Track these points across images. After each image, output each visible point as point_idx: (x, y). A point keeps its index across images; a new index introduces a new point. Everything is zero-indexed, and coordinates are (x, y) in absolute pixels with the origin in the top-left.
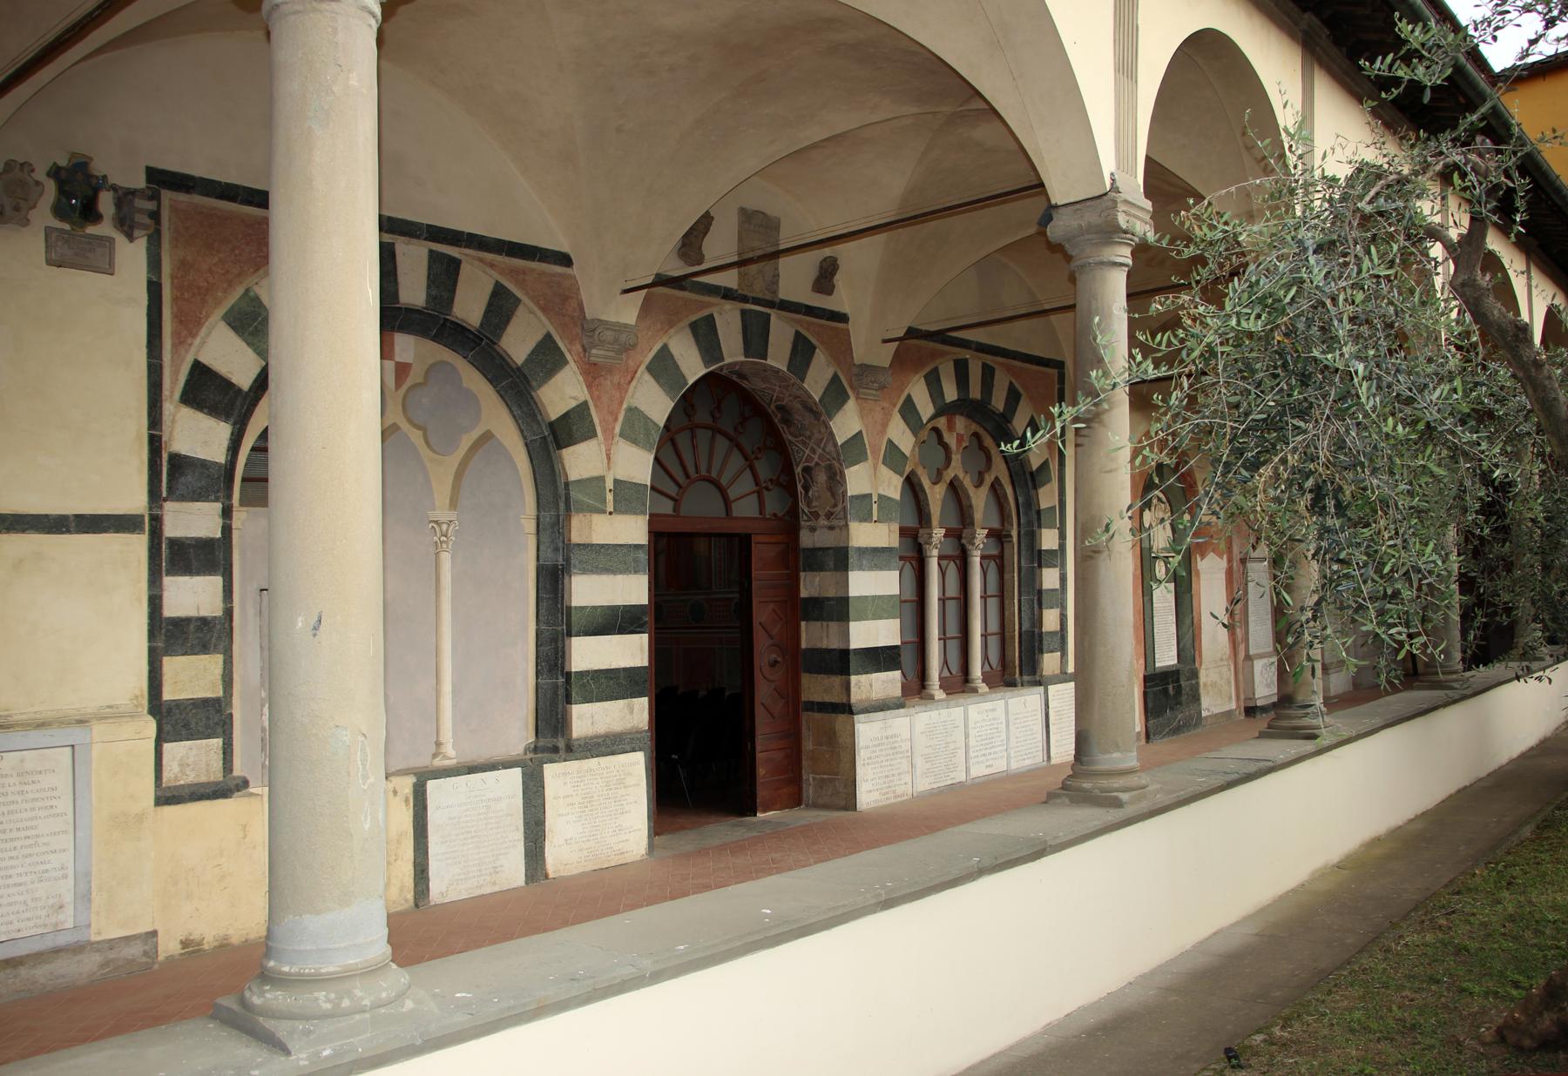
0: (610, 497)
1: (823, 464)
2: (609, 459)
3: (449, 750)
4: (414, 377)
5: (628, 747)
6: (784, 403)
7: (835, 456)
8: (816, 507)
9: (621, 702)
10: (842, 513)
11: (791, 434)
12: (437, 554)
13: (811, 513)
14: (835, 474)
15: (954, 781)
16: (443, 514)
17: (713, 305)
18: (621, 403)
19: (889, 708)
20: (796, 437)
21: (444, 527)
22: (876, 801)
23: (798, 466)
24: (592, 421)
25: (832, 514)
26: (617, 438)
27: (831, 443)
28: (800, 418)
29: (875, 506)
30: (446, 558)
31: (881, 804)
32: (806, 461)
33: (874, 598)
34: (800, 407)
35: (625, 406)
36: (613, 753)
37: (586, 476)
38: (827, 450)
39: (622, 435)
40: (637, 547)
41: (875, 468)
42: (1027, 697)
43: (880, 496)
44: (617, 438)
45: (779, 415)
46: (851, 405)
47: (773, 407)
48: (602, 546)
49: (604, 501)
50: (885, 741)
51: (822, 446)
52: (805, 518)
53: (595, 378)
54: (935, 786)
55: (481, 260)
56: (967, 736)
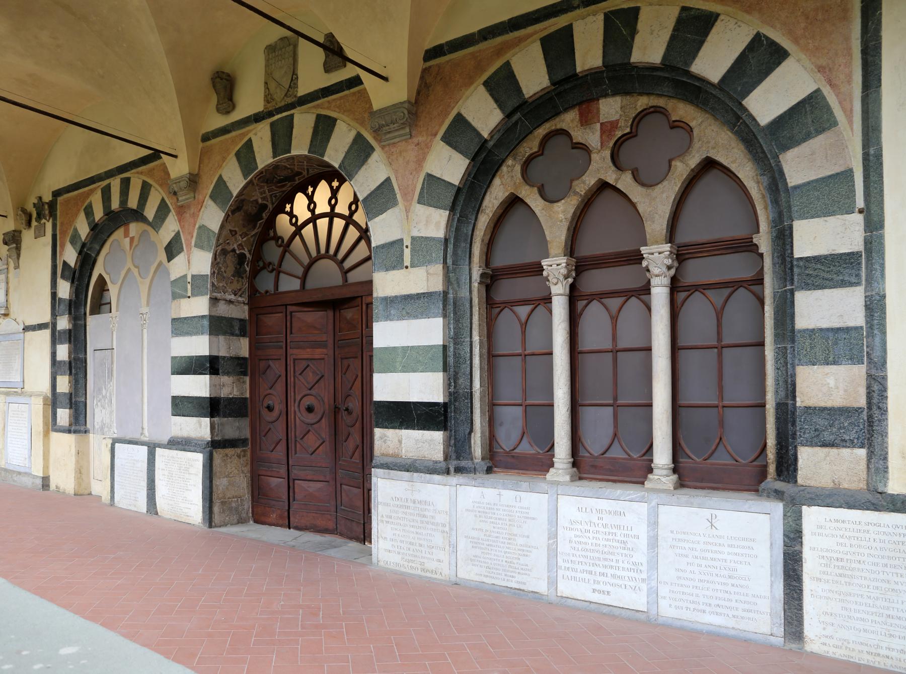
0: (189, 286)
2: (189, 263)
3: (146, 432)
4: (136, 240)
5: (192, 449)
9: (195, 419)
12: (142, 330)
15: (522, 587)
16: (144, 310)
17: (250, 131)
18: (195, 225)
19: (417, 470)
21: (145, 315)
22: (397, 564)
24: (181, 242)
26: (193, 248)
30: (145, 331)
31: (403, 569)
33: (405, 349)
35: (197, 226)
36: (185, 450)
37: (178, 276)
39: (196, 246)
40: (203, 317)
43: (414, 239)
44: (193, 248)
48: (185, 318)
49: (186, 290)
50: (411, 505)
53: (181, 215)
54: (488, 581)
55: (138, 173)
56: (553, 536)
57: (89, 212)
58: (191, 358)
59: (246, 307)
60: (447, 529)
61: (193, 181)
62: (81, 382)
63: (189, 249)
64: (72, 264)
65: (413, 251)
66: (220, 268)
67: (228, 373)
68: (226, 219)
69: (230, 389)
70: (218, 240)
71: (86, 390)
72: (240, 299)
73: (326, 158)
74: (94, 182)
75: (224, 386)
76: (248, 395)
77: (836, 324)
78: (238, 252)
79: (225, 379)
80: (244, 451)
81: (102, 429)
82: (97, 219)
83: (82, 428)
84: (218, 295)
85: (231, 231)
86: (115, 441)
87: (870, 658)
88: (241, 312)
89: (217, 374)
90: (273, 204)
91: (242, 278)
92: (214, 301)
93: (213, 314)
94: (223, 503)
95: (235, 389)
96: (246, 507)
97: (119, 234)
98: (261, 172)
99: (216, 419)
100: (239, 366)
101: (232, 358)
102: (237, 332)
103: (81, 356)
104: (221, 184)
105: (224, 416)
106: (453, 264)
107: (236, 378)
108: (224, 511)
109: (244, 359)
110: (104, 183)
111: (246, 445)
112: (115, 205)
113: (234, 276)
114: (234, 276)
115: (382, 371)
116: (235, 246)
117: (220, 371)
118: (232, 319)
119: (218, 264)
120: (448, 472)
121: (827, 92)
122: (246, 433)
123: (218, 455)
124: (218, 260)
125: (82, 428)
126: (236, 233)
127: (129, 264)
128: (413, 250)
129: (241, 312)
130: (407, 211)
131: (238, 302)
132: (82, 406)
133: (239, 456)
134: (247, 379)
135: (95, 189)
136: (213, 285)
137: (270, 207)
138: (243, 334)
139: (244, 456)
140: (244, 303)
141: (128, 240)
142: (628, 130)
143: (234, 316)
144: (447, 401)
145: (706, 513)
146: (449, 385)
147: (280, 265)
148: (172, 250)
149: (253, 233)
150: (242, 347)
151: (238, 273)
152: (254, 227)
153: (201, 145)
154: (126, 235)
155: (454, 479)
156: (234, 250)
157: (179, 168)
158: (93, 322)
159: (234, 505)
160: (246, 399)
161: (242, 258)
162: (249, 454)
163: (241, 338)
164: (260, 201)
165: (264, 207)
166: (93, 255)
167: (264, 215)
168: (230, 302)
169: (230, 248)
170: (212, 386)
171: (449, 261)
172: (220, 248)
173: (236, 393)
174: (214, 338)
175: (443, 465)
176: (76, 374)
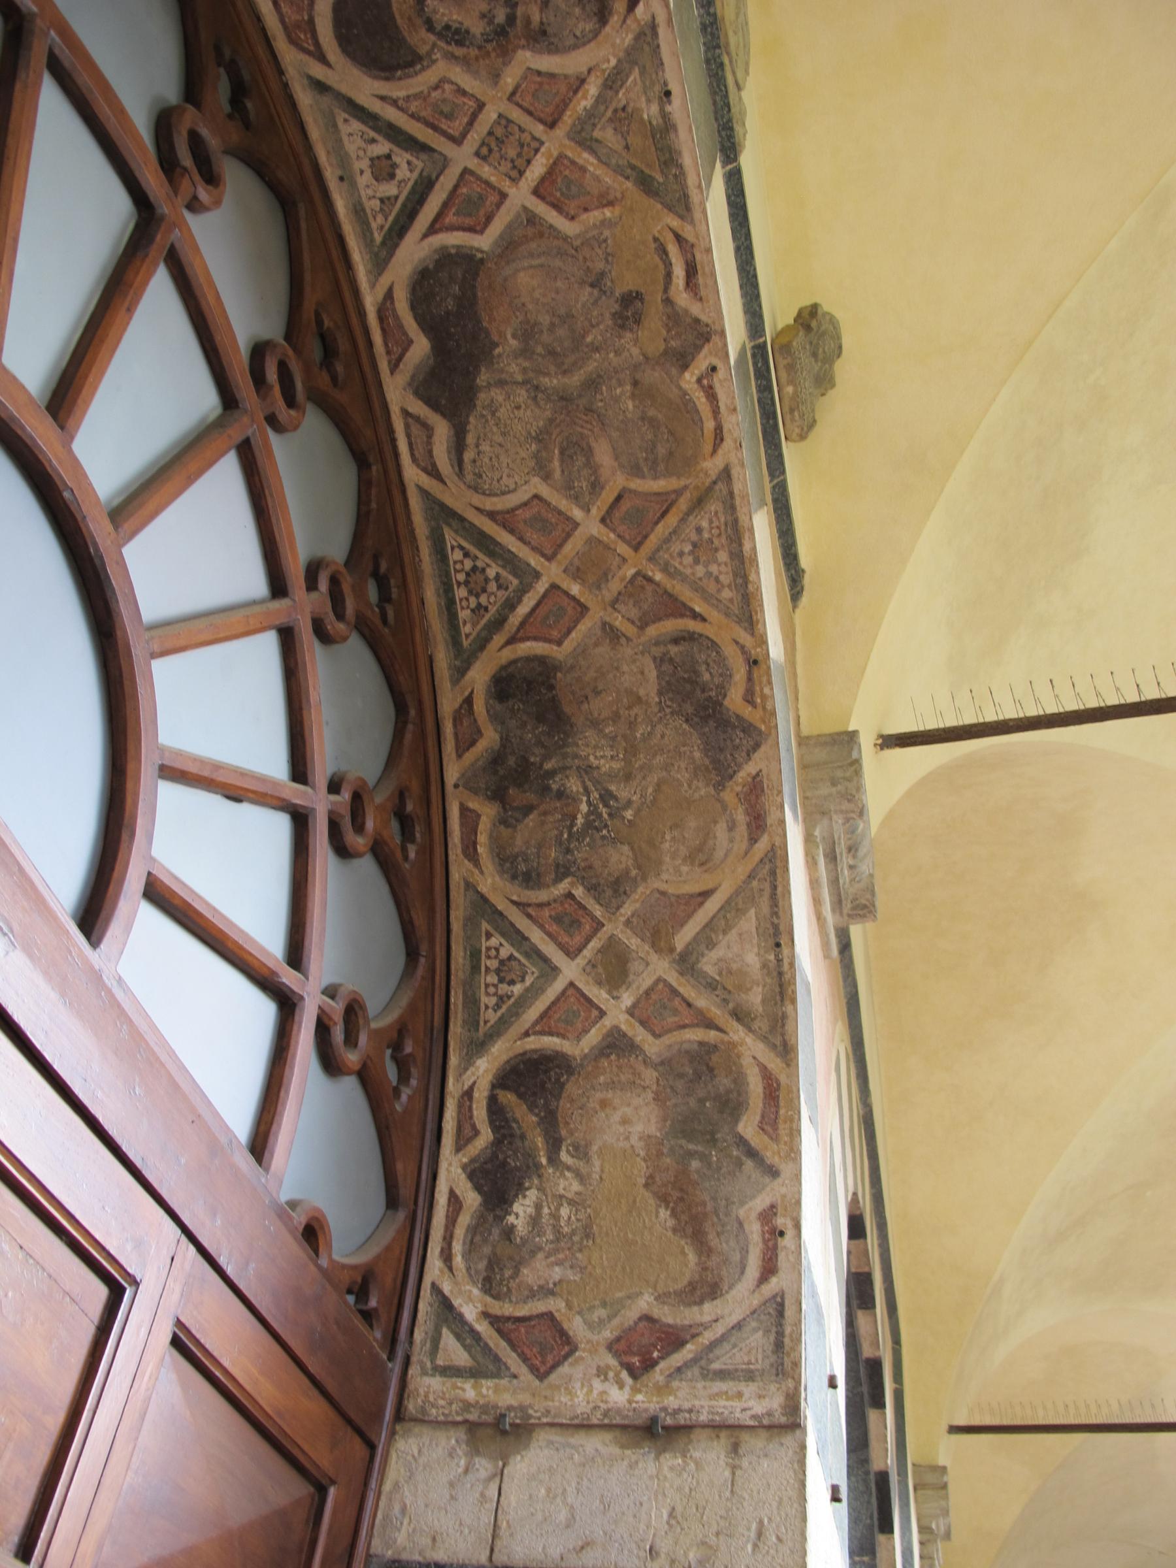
1: (653, 1047)
6: (559, 653)
7: (755, 999)
8: (547, 1291)
10: (756, 1342)
11: (507, 862)
13: (495, 1321)
14: (732, 1105)
20: (530, 879)
23: (477, 1047)
25: (674, 1339)
27: (749, 923)
28: (605, 761)
32: (544, 1025)
34: (650, 689)
38: (708, 964)
45: (490, 738)
47: (479, 676)
51: (683, 938)
52: (453, 1351)
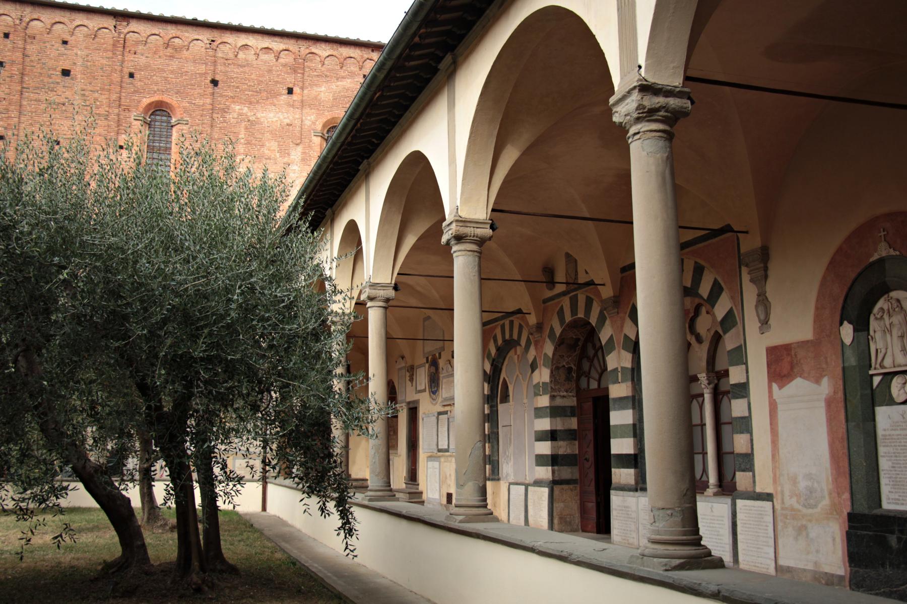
9: (545, 467)
16: (525, 401)
29: (620, 374)
39: (543, 365)
40: (547, 407)
41: (619, 352)
42: (715, 505)
43: (622, 368)
46: (608, 322)
48: (540, 408)
49: (540, 391)
57: (495, 341)
58: (542, 431)
59: (575, 399)
60: (635, 520)
61: (539, 327)
62: (496, 447)
63: (540, 366)
64: (488, 372)
65: (622, 374)
66: (556, 378)
67: (563, 440)
68: (556, 350)
69: (565, 449)
70: (552, 362)
71: (498, 452)
72: (570, 394)
73: (590, 321)
74: (497, 321)
75: (560, 447)
76: (577, 452)
77: (742, 416)
78: (566, 366)
79: (561, 443)
80: (576, 487)
81: (506, 477)
82: (499, 344)
83: (496, 477)
84: (555, 394)
85: (560, 356)
86: (510, 484)
87: (754, 568)
88: (572, 402)
89: (556, 440)
90: (583, 337)
91: (571, 381)
92: (553, 398)
93: (552, 405)
94: (561, 518)
95: (568, 449)
96: (577, 522)
97: (512, 353)
98: (568, 324)
99: (556, 468)
100: (570, 435)
101: (566, 431)
102: (570, 414)
103: (495, 430)
104: (552, 329)
105: (562, 465)
106: (637, 381)
107: (569, 442)
108: (561, 523)
109: (575, 430)
110: (502, 322)
111: (577, 483)
112: (507, 337)
113: (565, 381)
114: (565, 381)
115: (615, 438)
116: (564, 364)
117: (558, 439)
118: (566, 406)
119: (554, 375)
120: (636, 490)
121: (734, 308)
122: (576, 476)
123: (557, 489)
124: (554, 373)
125: (496, 477)
126: (563, 356)
127: (518, 373)
128: (622, 374)
129: (572, 402)
130: (619, 352)
131: (570, 396)
132: (496, 462)
133: (572, 490)
134: (577, 443)
135: (498, 325)
136: (552, 388)
137: (582, 339)
138: (573, 415)
139: (575, 490)
140: (573, 396)
141: (516, 357)
142: (693, 314)
143: (567, 405)
144: (636, 452)
145: (710, 504)
146: (638, 445)
147: (589, 373)
148: (534, 367)
149: (575, 354)
150: (573, 423)
151: (568, 379)
152: (575, 351)
153: (543, 305)
154: (516, 353)
155: (637, 494)
156: (564, 366)
157: (532, 320)
158: (501, 407)
159: (568, 520)
160: (576, 455)
161: (570, 370)
162: (578, 489)
163: (572, 418)
164: (574, 337)
165: (579, 339)
166: (500, 366)
167: (579, 343)
168: (564, 397)
169: (561, 365)
170: (553, 448)
171: (635, 380)
172: (554, 366)
173: (569, 451)
174: (553, 419)
175: (634, 487)
176: (492, 442)
